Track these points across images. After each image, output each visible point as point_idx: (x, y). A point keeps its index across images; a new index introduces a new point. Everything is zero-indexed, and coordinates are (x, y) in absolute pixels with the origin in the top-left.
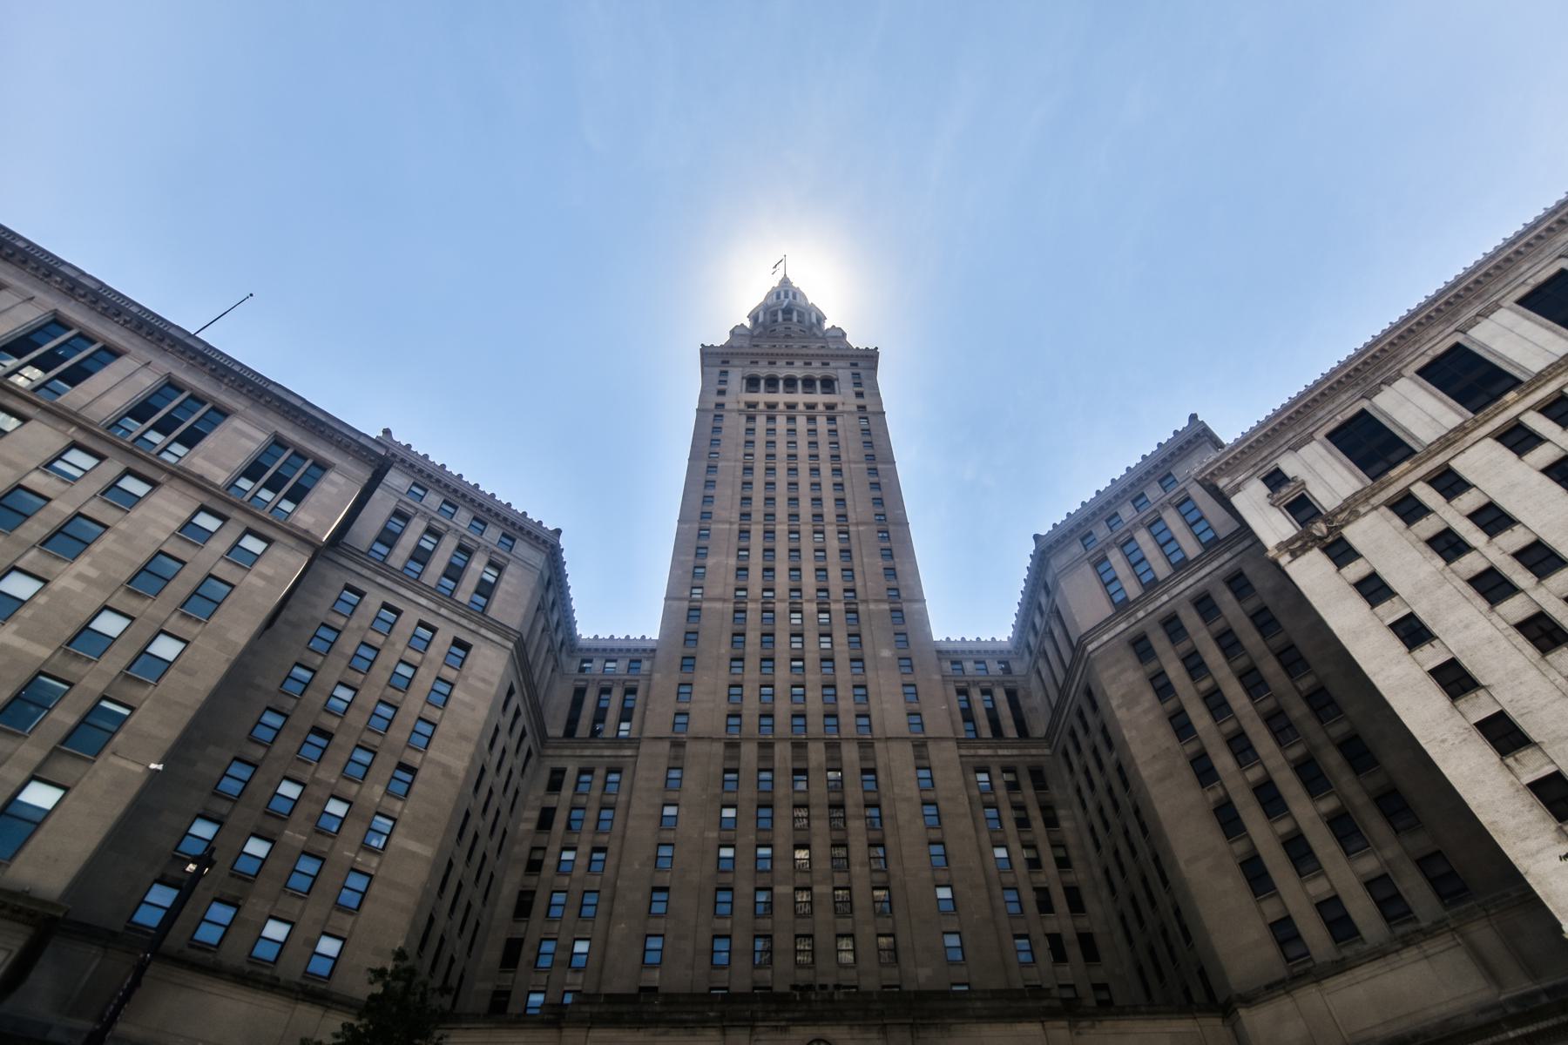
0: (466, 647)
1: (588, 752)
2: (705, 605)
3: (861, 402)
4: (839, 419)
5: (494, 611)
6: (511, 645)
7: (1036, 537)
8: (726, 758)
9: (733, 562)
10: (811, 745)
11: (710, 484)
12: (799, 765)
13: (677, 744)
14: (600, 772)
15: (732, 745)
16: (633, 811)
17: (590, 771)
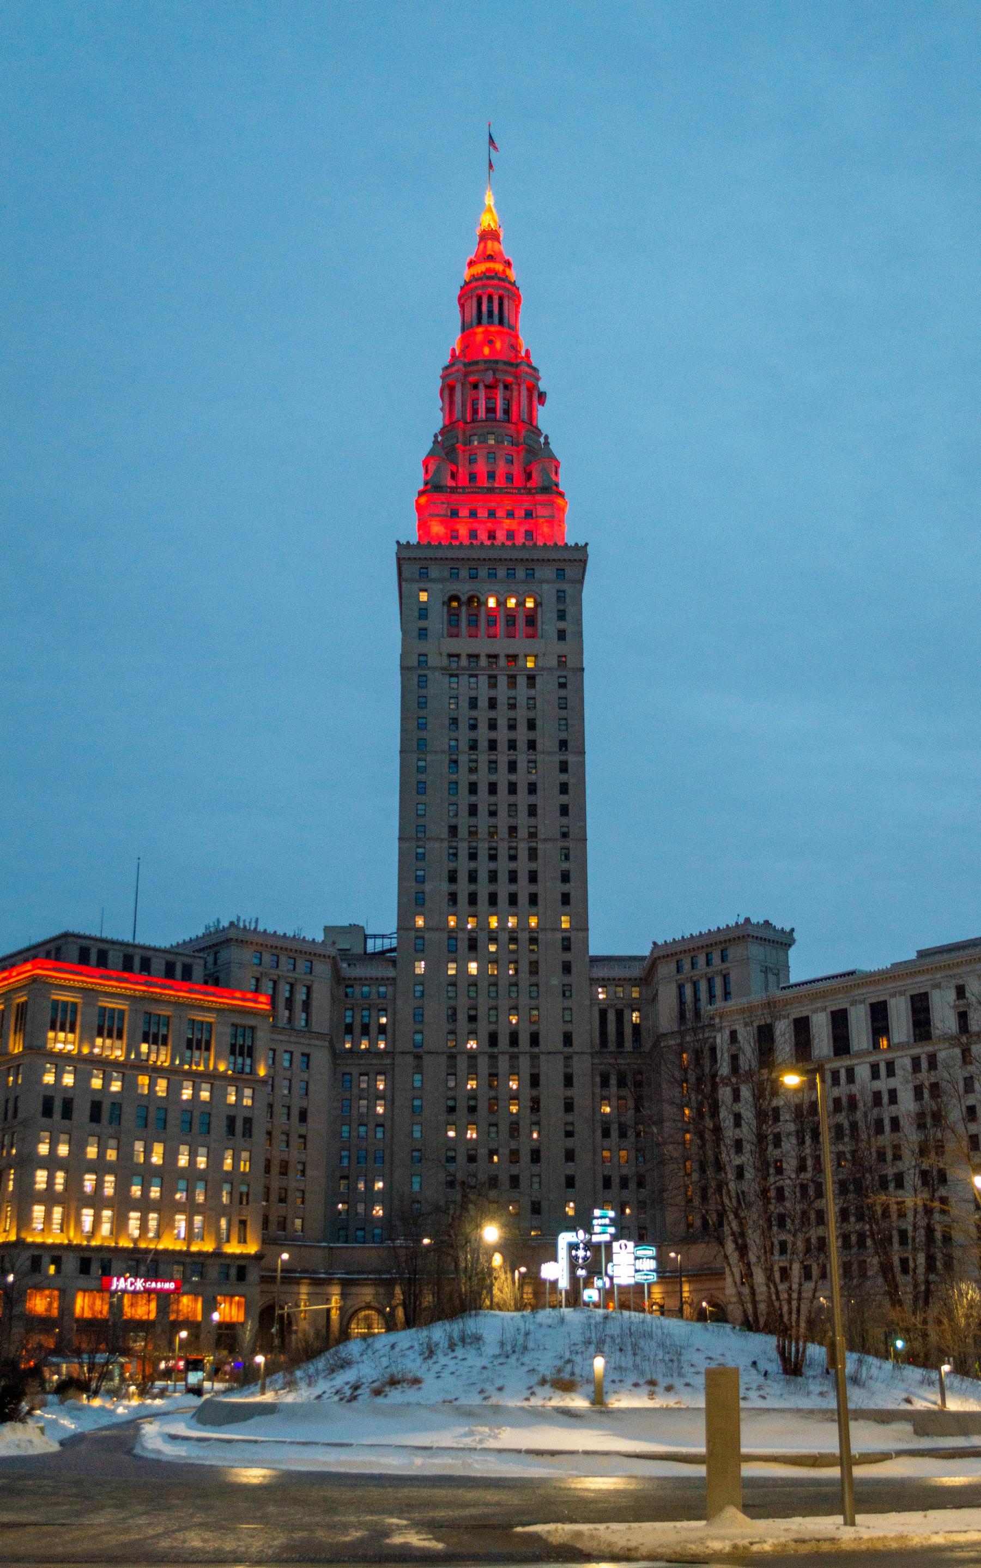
0: (307, 1056)
1: (362, 1062)
2: (427, 936)
3: (560, 648)
4: (539, 680)
5: (315, 1028)
6: (327, 1044)
7: (655, 943)
8: (448, 1067)
9: (445, 887)
10: (501, 1057)
11: (421, 788)
12: (494, 1071)
13: (418, 1057)
14: (372, 1076)
15: (452, 1057)
16: (397, 1104)
17: (367, 1074)
